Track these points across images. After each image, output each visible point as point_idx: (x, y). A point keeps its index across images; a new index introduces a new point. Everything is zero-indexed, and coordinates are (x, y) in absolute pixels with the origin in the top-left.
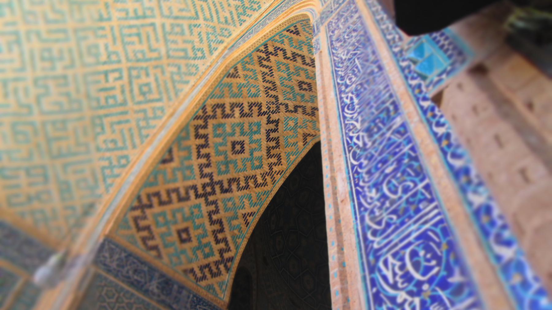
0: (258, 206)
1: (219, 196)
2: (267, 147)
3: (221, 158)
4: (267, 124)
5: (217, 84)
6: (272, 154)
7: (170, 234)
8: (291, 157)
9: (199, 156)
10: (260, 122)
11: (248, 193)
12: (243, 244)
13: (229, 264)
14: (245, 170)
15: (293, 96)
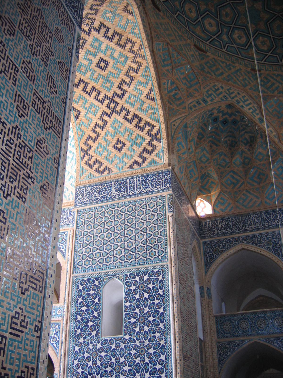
0: (150, 82)
1: (121, 102)
2: (116, 44)
3: (101, 80)
4: (99, 33)
6: (123, 44)
7: (111, 153)
8: (135, 31)
9: (90, 94)
10: (94, 37)
11: (136, 81)
13: (158, 136)
14: (121, 71)
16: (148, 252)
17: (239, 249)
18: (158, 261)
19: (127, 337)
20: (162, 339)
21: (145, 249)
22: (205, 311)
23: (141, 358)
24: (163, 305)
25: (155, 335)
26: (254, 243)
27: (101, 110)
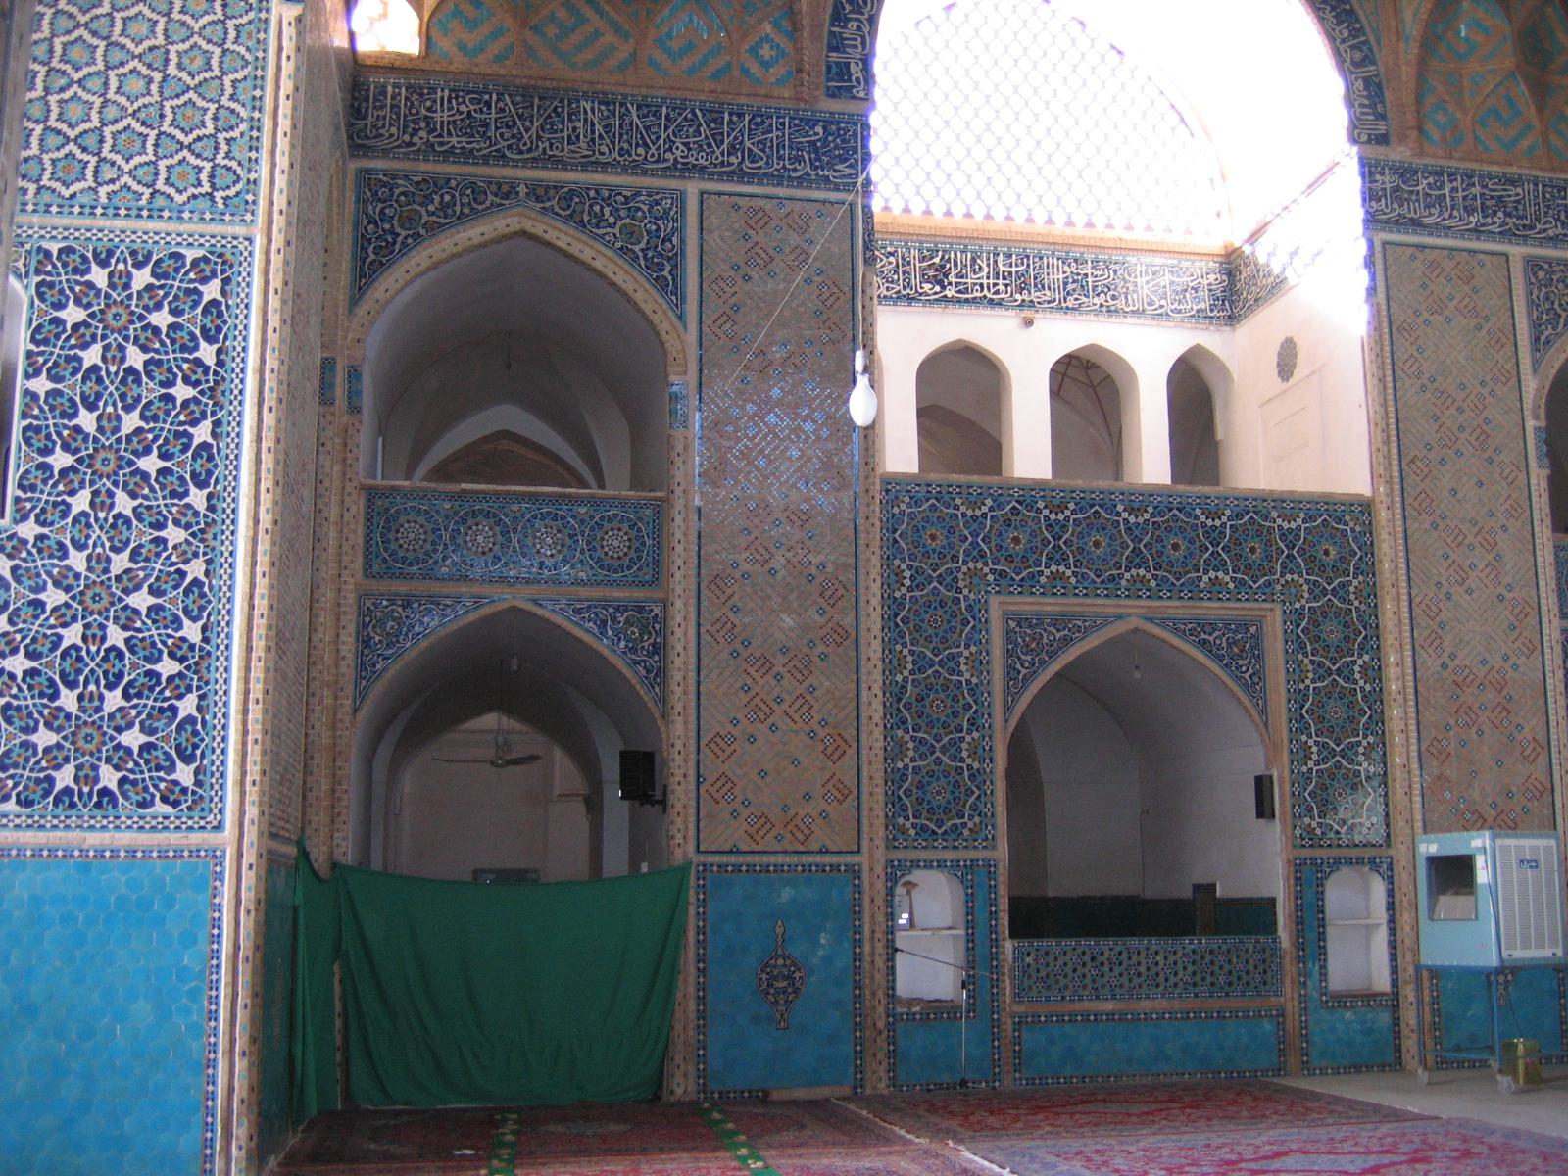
16: (162, 164)
17: (507, 231)
18: (207, 216)
19: (29, 530)
20: (196, 555)
21: (150, 148)
22: (328, 463)
23: (87, 627)
24: (213, 413)
25: (163, 534)
26: (575, 220)
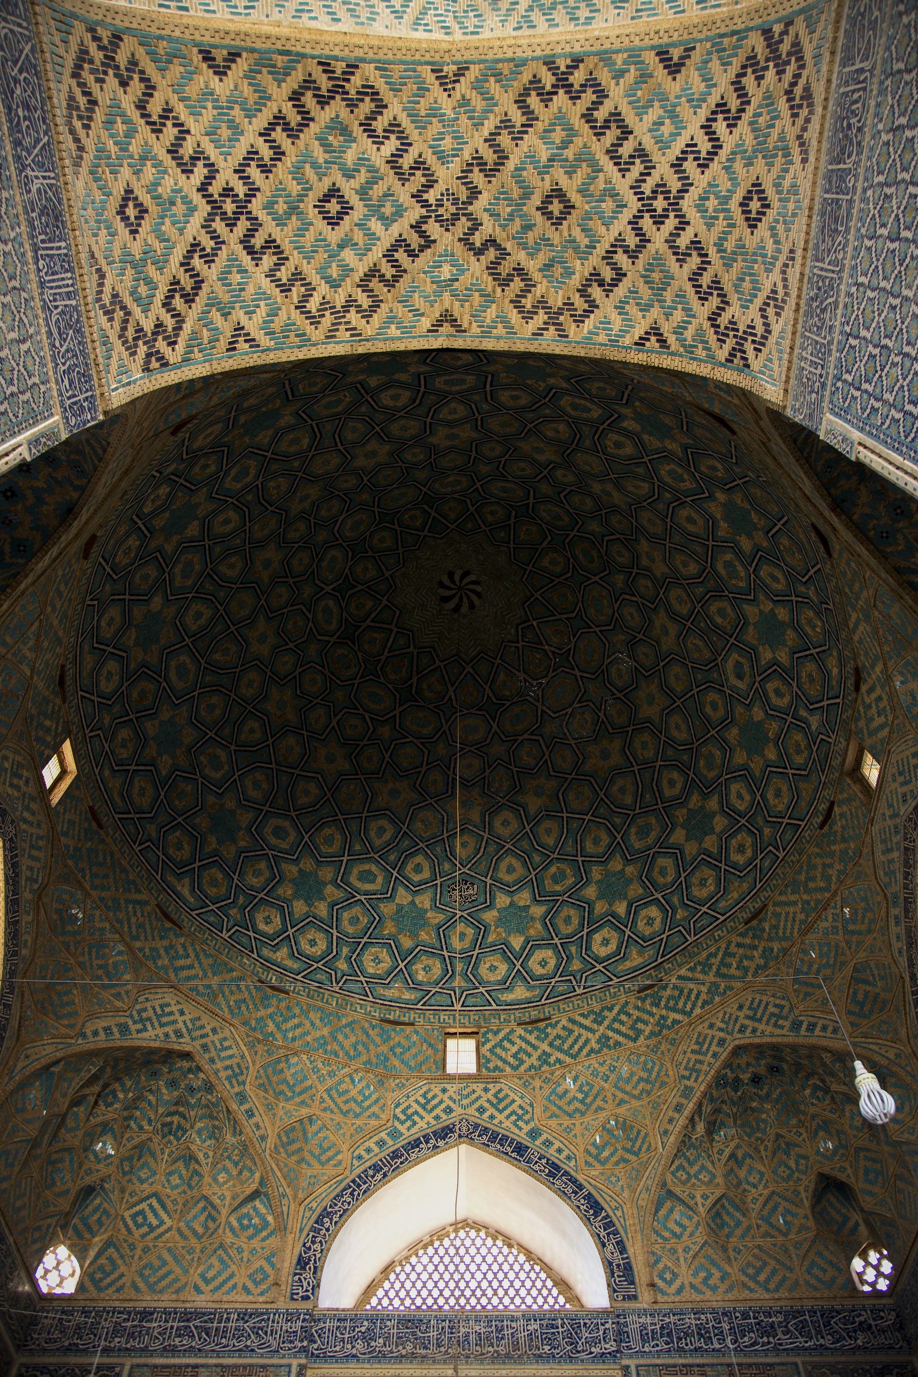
1: (233, 238)
3: (295, 188)
4: (412, 227)
5: (409, 58)
8: (393, 327)
10: (406, 210)
12: (198, 370)
14: (308, 259)
15: (511, 214)
27: (221, 164)
